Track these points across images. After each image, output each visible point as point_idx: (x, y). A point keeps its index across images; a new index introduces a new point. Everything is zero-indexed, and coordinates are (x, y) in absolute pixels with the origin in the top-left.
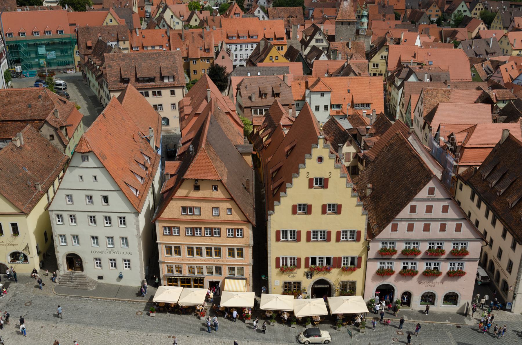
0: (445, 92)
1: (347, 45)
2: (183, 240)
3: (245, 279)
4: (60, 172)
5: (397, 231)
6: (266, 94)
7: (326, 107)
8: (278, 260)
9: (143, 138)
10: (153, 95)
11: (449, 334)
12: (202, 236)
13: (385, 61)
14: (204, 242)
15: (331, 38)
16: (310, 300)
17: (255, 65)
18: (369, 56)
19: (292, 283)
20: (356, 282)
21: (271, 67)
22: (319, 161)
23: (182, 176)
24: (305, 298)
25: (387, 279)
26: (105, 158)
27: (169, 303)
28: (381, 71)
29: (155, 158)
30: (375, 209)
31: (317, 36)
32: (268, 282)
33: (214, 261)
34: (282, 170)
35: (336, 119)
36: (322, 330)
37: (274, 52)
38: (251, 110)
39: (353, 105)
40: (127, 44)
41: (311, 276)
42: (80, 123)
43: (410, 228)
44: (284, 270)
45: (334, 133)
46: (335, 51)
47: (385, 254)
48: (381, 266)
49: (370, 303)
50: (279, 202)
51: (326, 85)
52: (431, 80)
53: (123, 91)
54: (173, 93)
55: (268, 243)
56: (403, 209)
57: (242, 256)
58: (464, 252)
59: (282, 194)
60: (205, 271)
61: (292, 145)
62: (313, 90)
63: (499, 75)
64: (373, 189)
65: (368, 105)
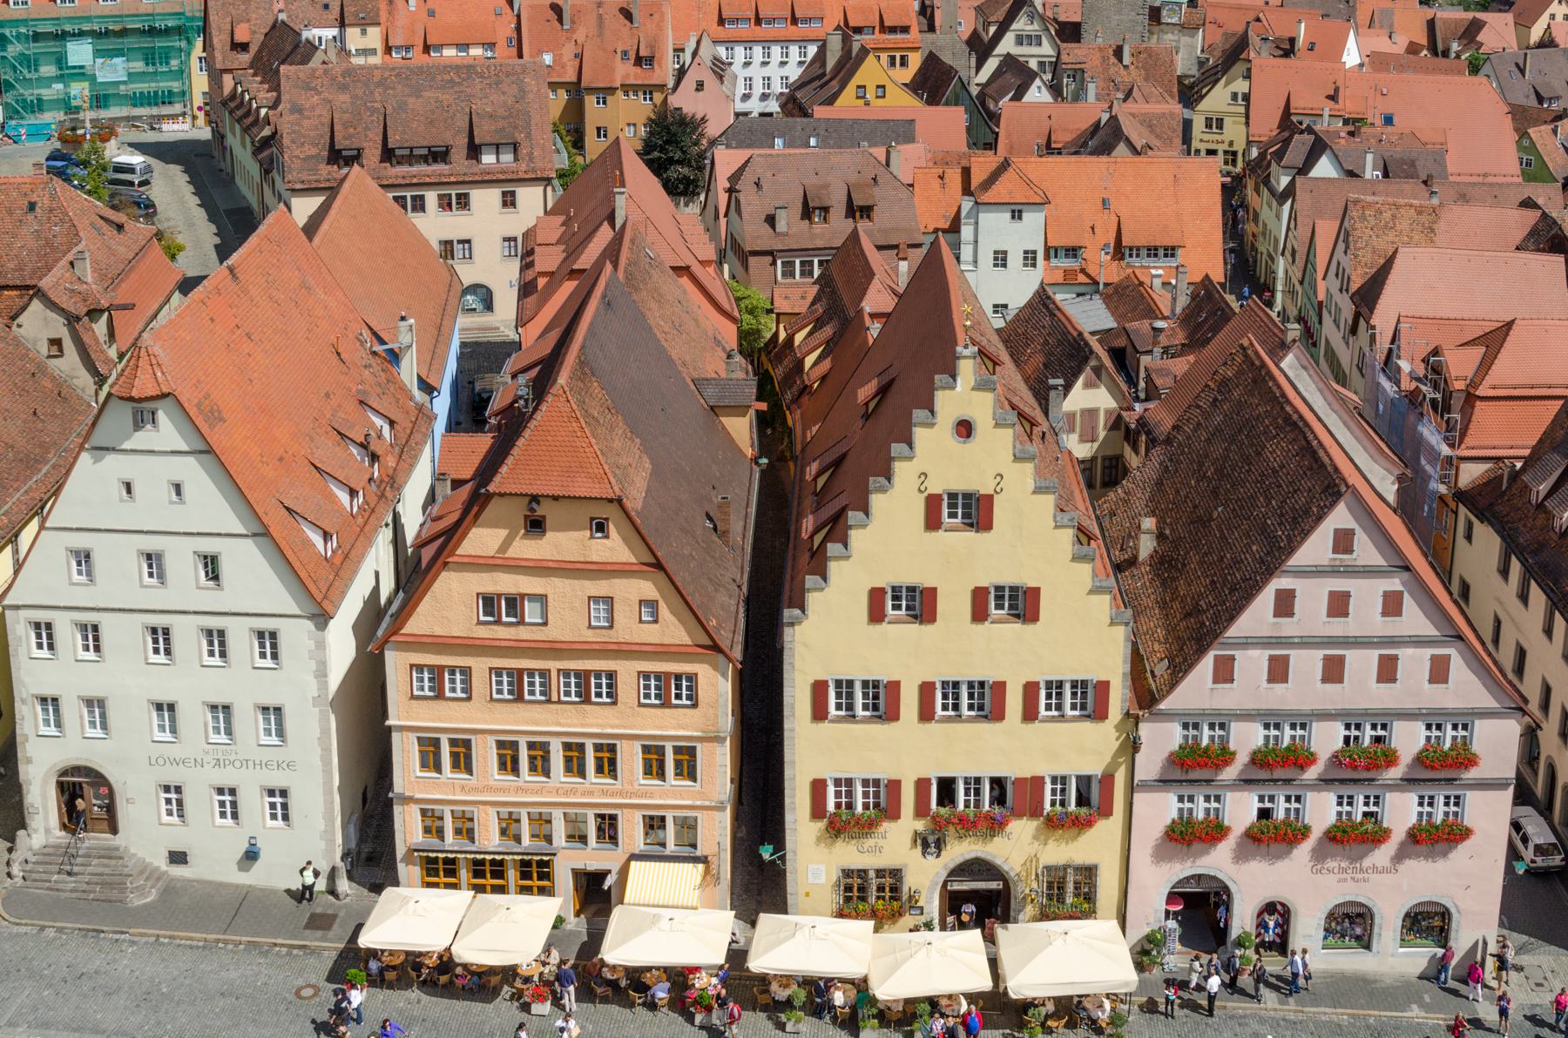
1: (1118, 52)
6: (826, 210)
7: (1030, 258)
8: (818, 787)
13: (1242, 110)
14: (558, 721)
15: (1070, 32)
17: (804, 113)
18: (1189, 94)
21: (855, 121)
30: (1163, 605)
31: (1021, 24)
37: (871, 72)
39: (1119, 251)
40: (374, 37)
41: (940, 845)
45: (1046, 342)
46: (1078, 74)
47: (1194, 765)
48: (1181, 810)
52: (1386, 175)
53: (332, 191)
61: (886, 379)
62: (984, 198)
64: (1160, 537)
65: (1170, 252)
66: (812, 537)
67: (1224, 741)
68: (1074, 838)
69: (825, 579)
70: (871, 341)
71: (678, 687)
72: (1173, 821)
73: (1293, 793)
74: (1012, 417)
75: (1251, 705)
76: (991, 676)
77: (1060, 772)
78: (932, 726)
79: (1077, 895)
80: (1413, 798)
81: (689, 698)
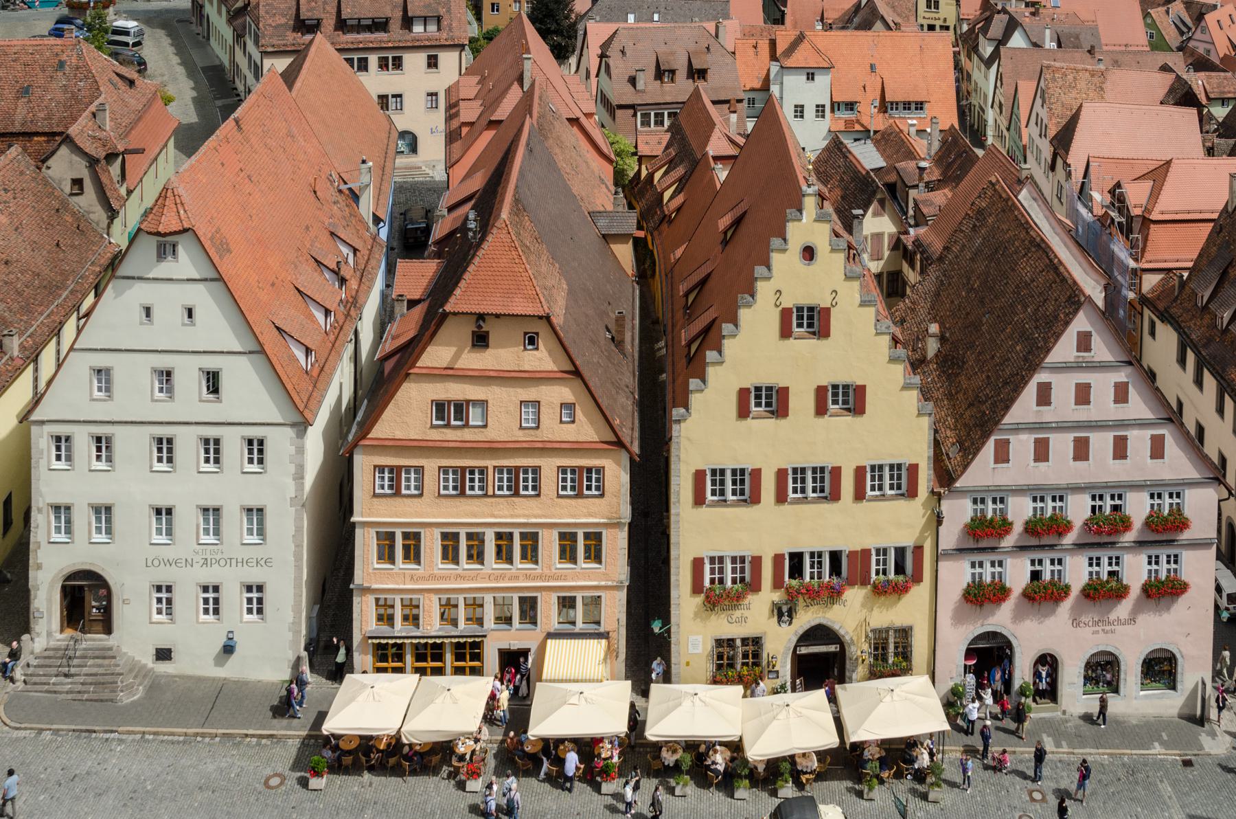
0: (1092, 76)
2: (431, 512)
3: (604, 636)
4: (85, 296)
5: (1008, 461)
8: (698, 564)
9: (340, 191)
10: (381, 67)
11: (1166, 789)
12: (486, 495)
19: (738, 643)
22: (805, 258)
23: (442, 305)
25: (993, 614)
26: (225, 248)
27: (371, 738)
28: (945, 20)
29: (371, 250)
32: (669, 643)
34: (711, 283)
35: (845, 142)
36: (824, 802)
38: (635, 115)
42: (166, 145)
43: (1042, 452)
44: (716, 599)
47: (984, 534)
49: (952, 699)
50: (704, 381)
51: (818, 52)
54: (433, 63)
55: (673, 511)
56: (1019, 395)
57: (598, 558)
58: (1177, 522)
59: (711, 355)
60: (489, 613)
61: (738, 212)
63: (1206, 37)
64: (942, 339)
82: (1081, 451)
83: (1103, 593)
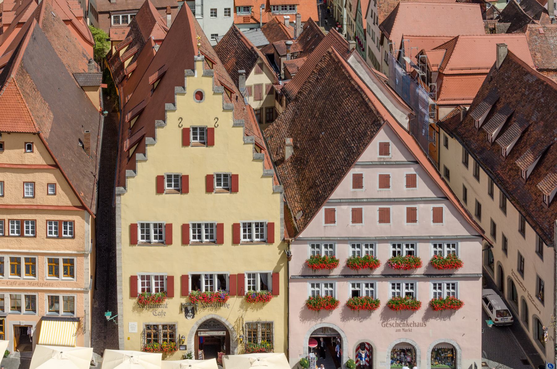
3: (77, 320)
5: (334, 222)
16: (193, 362)
20: (272, 323)
24: (184, 358)
30: (298, 183)
33: (23, 284)
43: (357, 217)
44: (145, 301)
47: (319, 267)
48: (313, 292)
66: (128, 150)
67: (333, 254)
68: (261, 308)
69: (135, 172)
70: (155, 53)
71: (66, 228)
72: (310, 298)
73: (369, 282)
74: (222, 89)
75: (344, 235)
76: (216, 220)
77: (252, 271)
78: (188, 247)
79: (263, 339)
80: (430, 285)
81: (71, 233)
82: (384, 216)
83: (402, 307)
